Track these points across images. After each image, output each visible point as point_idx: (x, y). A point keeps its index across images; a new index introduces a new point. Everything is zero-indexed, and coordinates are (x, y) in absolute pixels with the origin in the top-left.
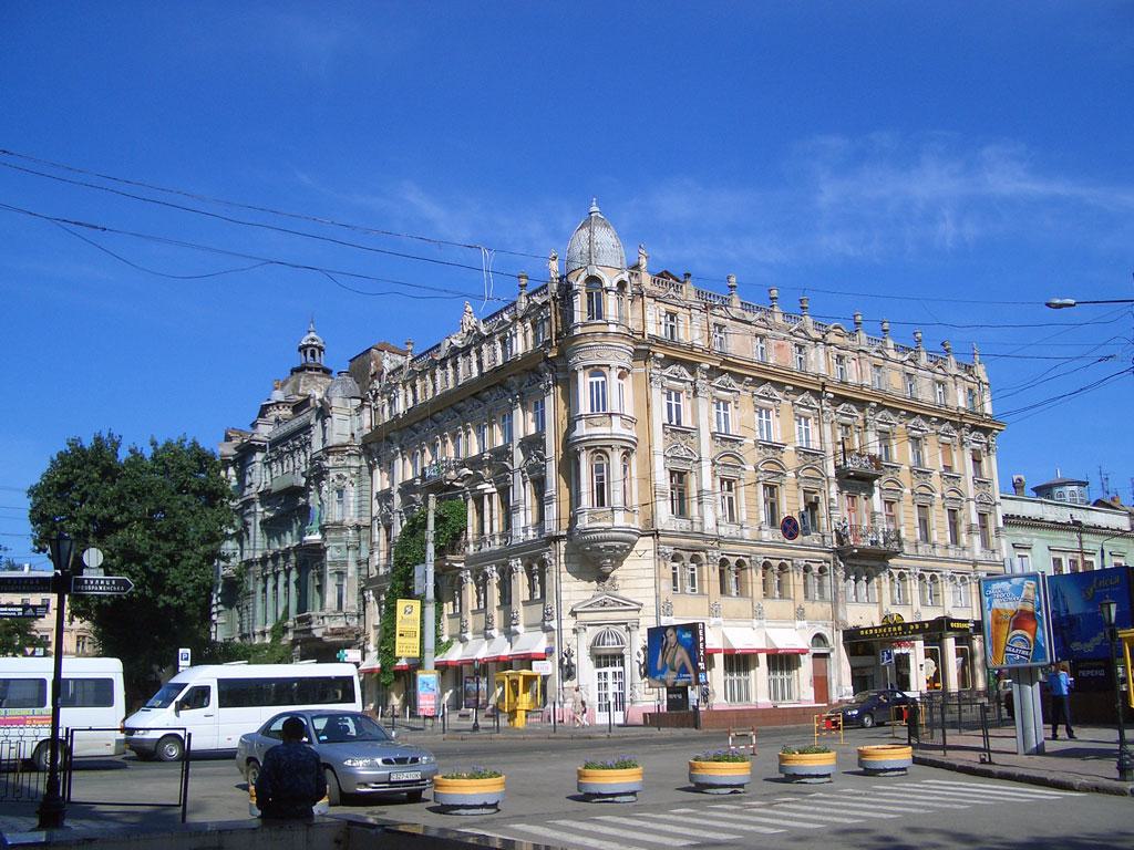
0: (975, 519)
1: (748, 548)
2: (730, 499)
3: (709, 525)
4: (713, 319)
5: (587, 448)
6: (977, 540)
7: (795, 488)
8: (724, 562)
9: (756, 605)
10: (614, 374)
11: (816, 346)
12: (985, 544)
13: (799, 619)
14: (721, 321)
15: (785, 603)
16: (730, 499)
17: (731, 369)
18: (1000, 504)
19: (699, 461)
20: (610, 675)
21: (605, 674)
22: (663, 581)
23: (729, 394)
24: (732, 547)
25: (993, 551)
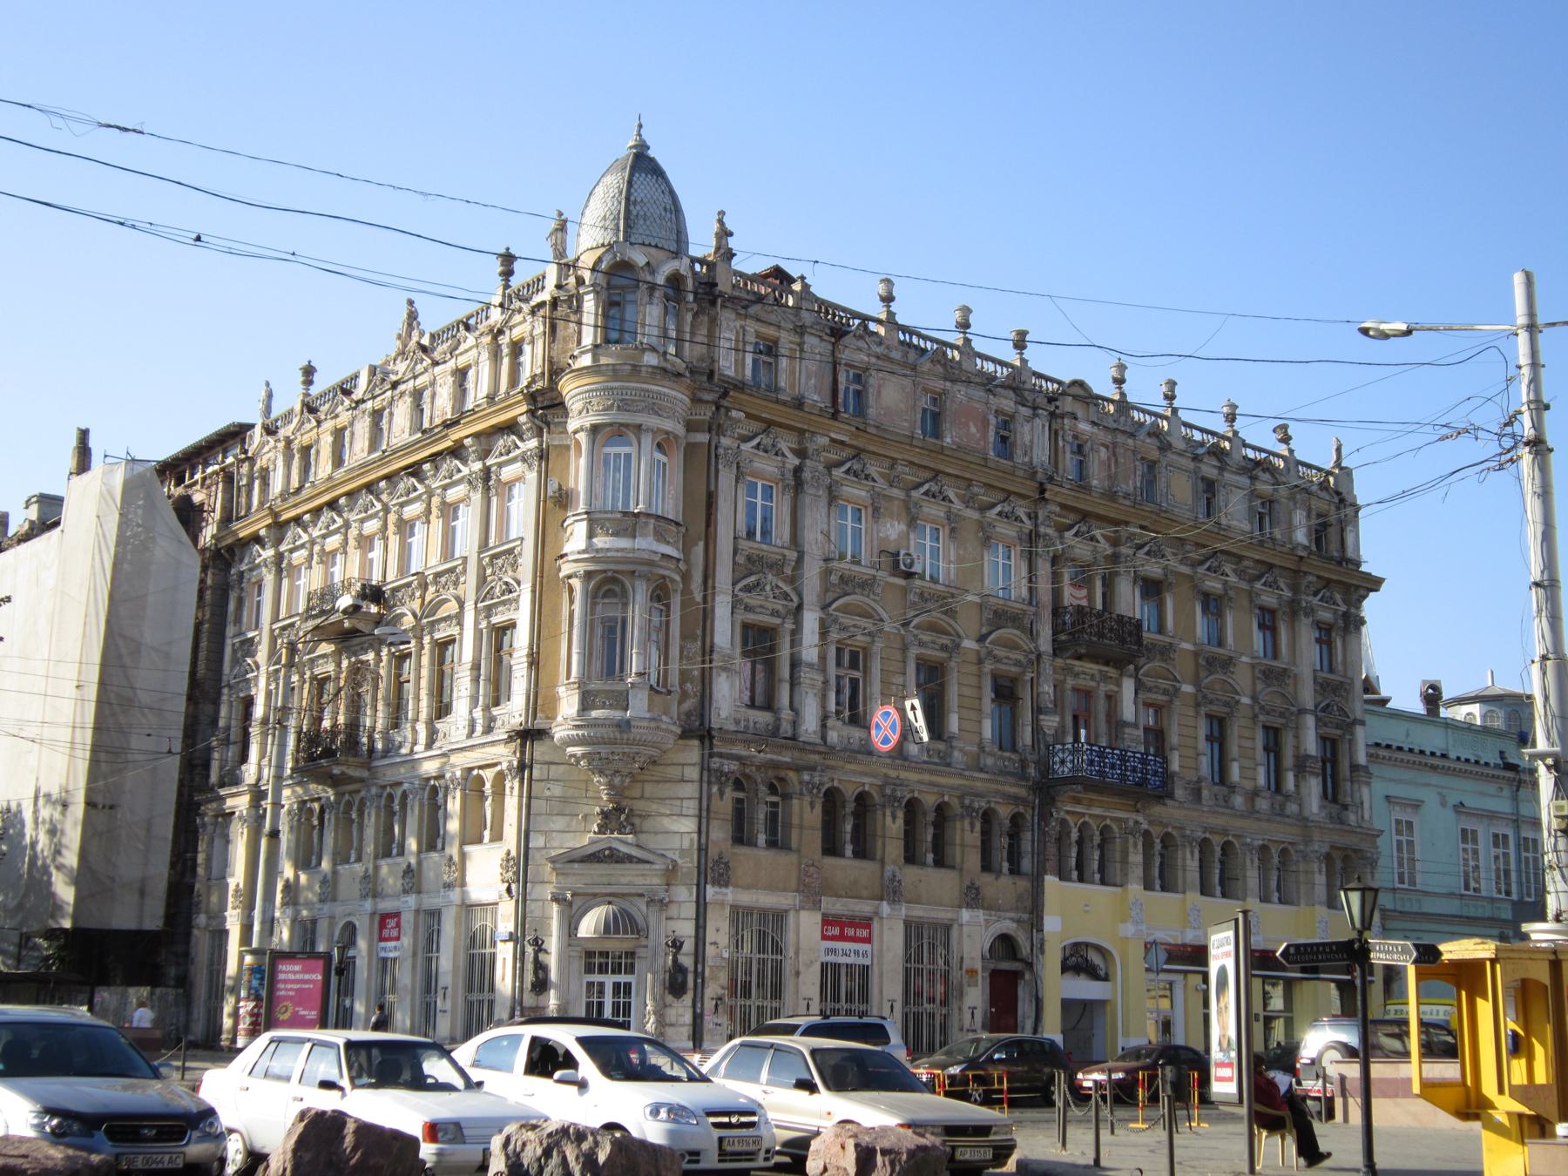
0: (1311, 745)
2: (854, 683)
3: (810, 724)
6: (1313, 786)
8: (832, 799)
9: (888, 874)
10: (647, 441)
11: (1036, 415)
12: (1332, 794)
13: (969, 906)
15: (868, 867)
16: (854, 683)
18: (1362, 723)
19: (800, 607)
20: (609, 990)
21: (602, 984)
22: (714, 824)
25: (1345, 807)
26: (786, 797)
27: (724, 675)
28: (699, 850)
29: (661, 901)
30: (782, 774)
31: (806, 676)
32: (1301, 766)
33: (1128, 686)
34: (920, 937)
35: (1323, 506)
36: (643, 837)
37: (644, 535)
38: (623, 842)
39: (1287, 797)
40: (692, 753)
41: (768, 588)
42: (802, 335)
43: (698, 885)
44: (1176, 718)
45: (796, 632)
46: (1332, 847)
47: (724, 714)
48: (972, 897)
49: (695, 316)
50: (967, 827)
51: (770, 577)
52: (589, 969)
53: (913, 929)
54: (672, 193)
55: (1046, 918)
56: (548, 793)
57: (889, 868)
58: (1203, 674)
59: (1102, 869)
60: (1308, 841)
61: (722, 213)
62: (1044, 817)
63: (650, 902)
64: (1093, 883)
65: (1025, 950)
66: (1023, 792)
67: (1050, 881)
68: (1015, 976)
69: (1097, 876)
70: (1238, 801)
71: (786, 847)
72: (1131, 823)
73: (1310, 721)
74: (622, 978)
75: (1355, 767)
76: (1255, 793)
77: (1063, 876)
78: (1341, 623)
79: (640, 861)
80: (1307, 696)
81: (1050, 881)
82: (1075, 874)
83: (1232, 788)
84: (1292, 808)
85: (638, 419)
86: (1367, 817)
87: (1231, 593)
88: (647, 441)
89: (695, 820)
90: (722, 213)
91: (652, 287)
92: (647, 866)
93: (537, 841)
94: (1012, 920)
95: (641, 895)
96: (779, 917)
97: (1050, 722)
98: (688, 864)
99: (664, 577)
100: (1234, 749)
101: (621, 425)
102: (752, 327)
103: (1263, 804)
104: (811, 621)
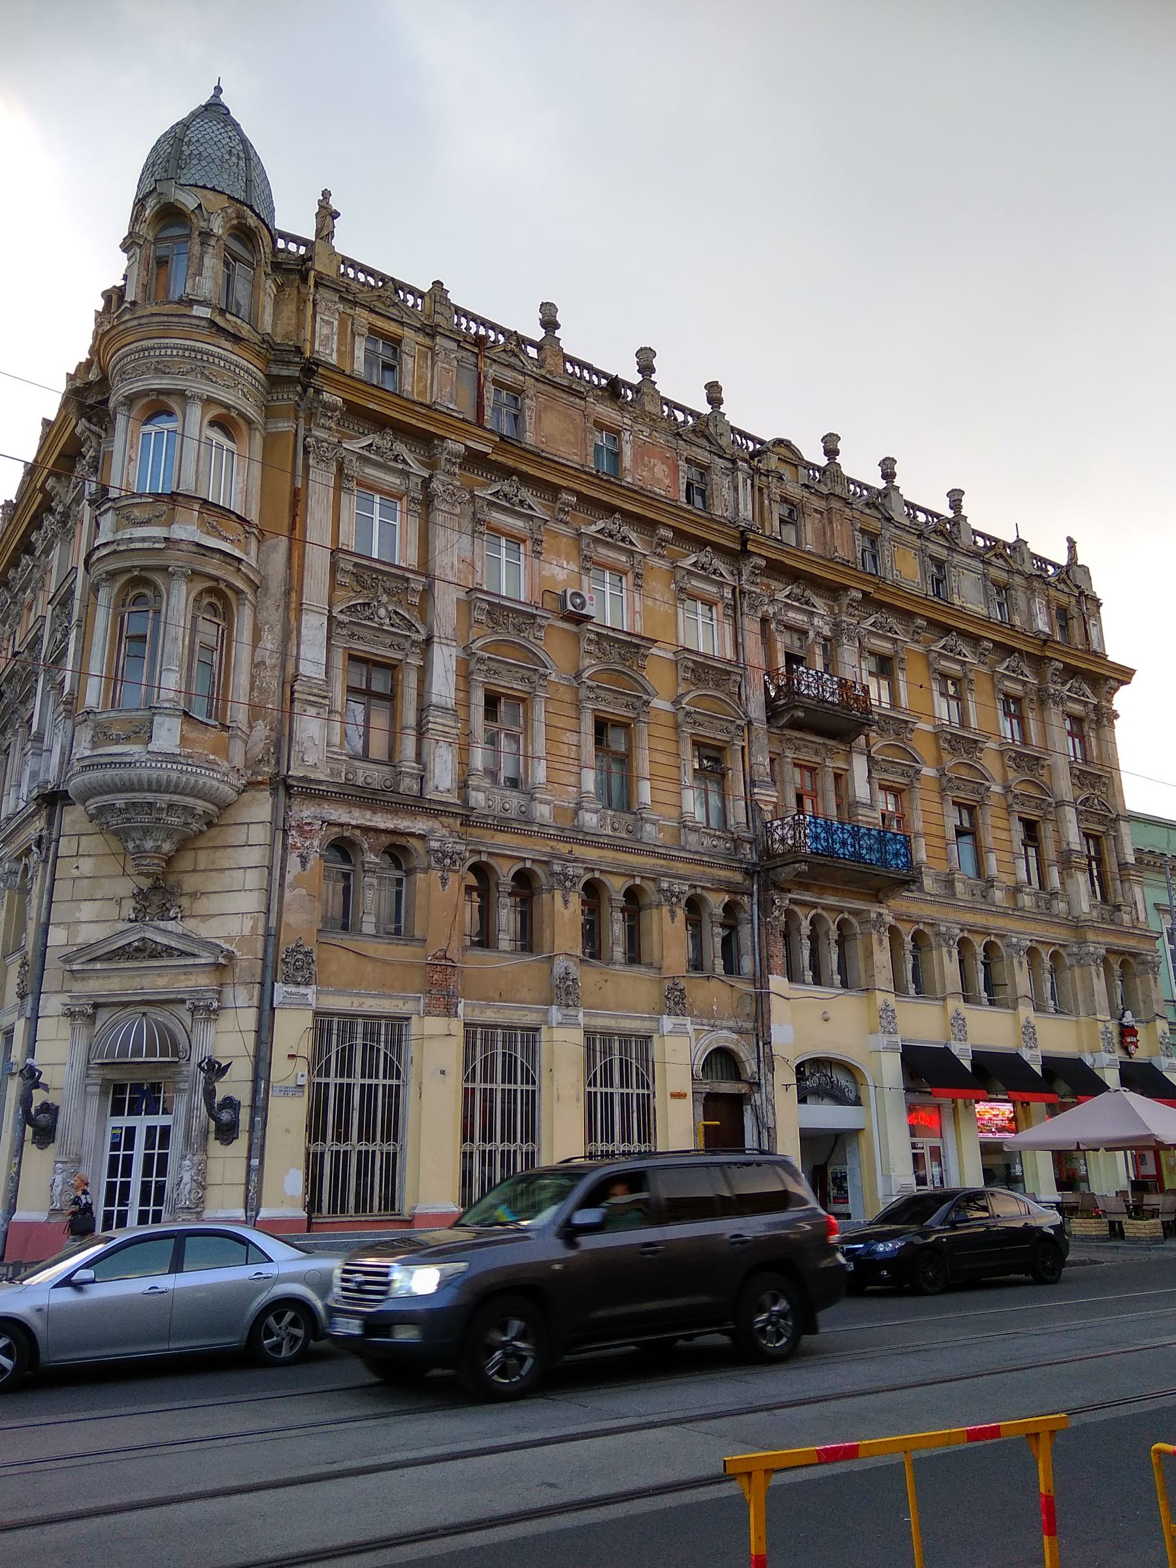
0: (1074, 838)
1: (546, 847)
4: (492, 371)
5: (112, 575)
7: (669, 733)
10: (195, 414)
14: (509, 376)
17: (524, 468)
19: (429, 641)
23: (520, 523)
24: (501, 838)
25: (1117, 908)
26: (410, 872)
27: (312, 711)
28: (267, 935)
29: (207, 1008)
30: (401, 841)
31: (437, 722)
32: (1066, 861)
33: (860, 766)
34: (607, 1051)
35: (1064, 599)
36: (191, 925)
37: (187, 523)
38: (161, 933)
39: (1054, 895)
40: (261, 807)
41: (382, 612)
42: (432, 337)
43: (262, 984)
44: (919, 805)
45: (424, 672)
46: (1108, 951)
47: (310, 759)
48: (675, 1001)
49: (280, 288)
50: (666, 915)
51: (384, 599)
52: (117, 1111)
53: (596, 1042)
54: (244, 141)
55: (774, 1028)
56: (75, 873)
57: (560, 964)
58: (946, 757)
59: (843, 969)
60: (1082, 942)
61: (326, 194)
62: (765, 906)
63: (194, 1010)
64: (832, 986)
65: (750, 1067)
66: (738, 877)
67: (777, 982)
68: (736, 1103)
69: (837, 978)
70: (998, 895)
71: (412, 939)
72: (873, 915)
73: (1070, 813)
74: (159, 1120)
75: (1123, 866)
76: (1017, 890)
77: (792, 975)
78: (1093, 716)
79: (183, 954)
80: (1064, 787)
81: (777, 982)
82: (809, 976)
83: (990, 883)
84: (1060, 906)
85: (180, 384)
86: (1142, 919)
87: (971, 676)
88: (195, 414)
89: (263, 896)
90: (326, 194)
91: (206, 235)
92: (190, 961)
93: (57, 936)
94: (730, 1029)
95: (183, 1001)
96: (398, 1024)
97: (767, 796)
98: (248, 958)
99: (216, 579)
100: (988, 840)
101: (160, 392)
102: (364, 317)
103: (1027, 900)
104: (444, 660)
